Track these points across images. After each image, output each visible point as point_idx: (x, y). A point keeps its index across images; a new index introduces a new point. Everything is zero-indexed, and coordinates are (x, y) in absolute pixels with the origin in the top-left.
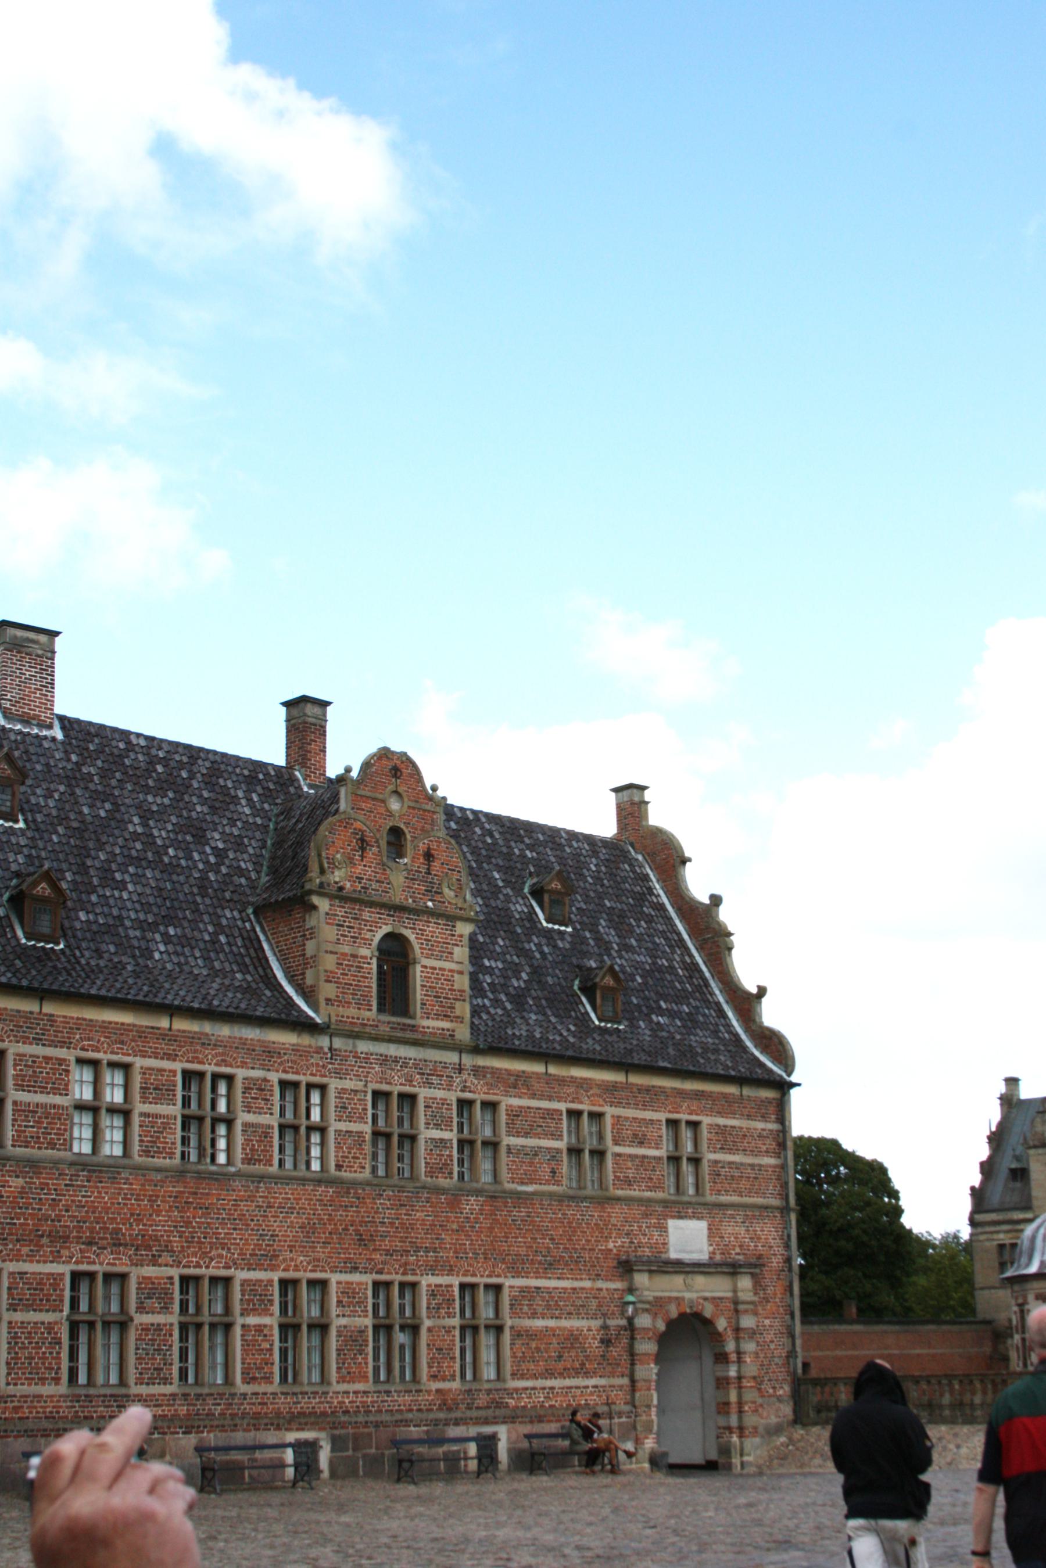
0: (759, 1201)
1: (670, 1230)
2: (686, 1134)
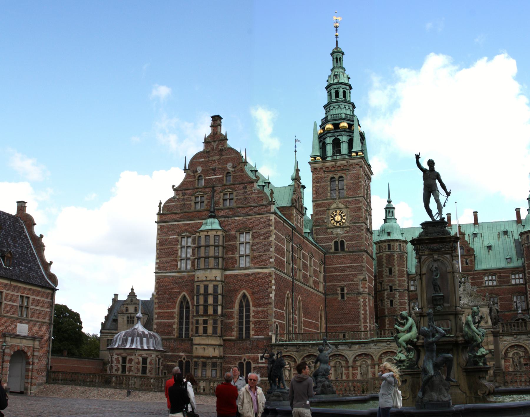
0: (44, 321)
1: (18, 326)
2: (25, 300)
